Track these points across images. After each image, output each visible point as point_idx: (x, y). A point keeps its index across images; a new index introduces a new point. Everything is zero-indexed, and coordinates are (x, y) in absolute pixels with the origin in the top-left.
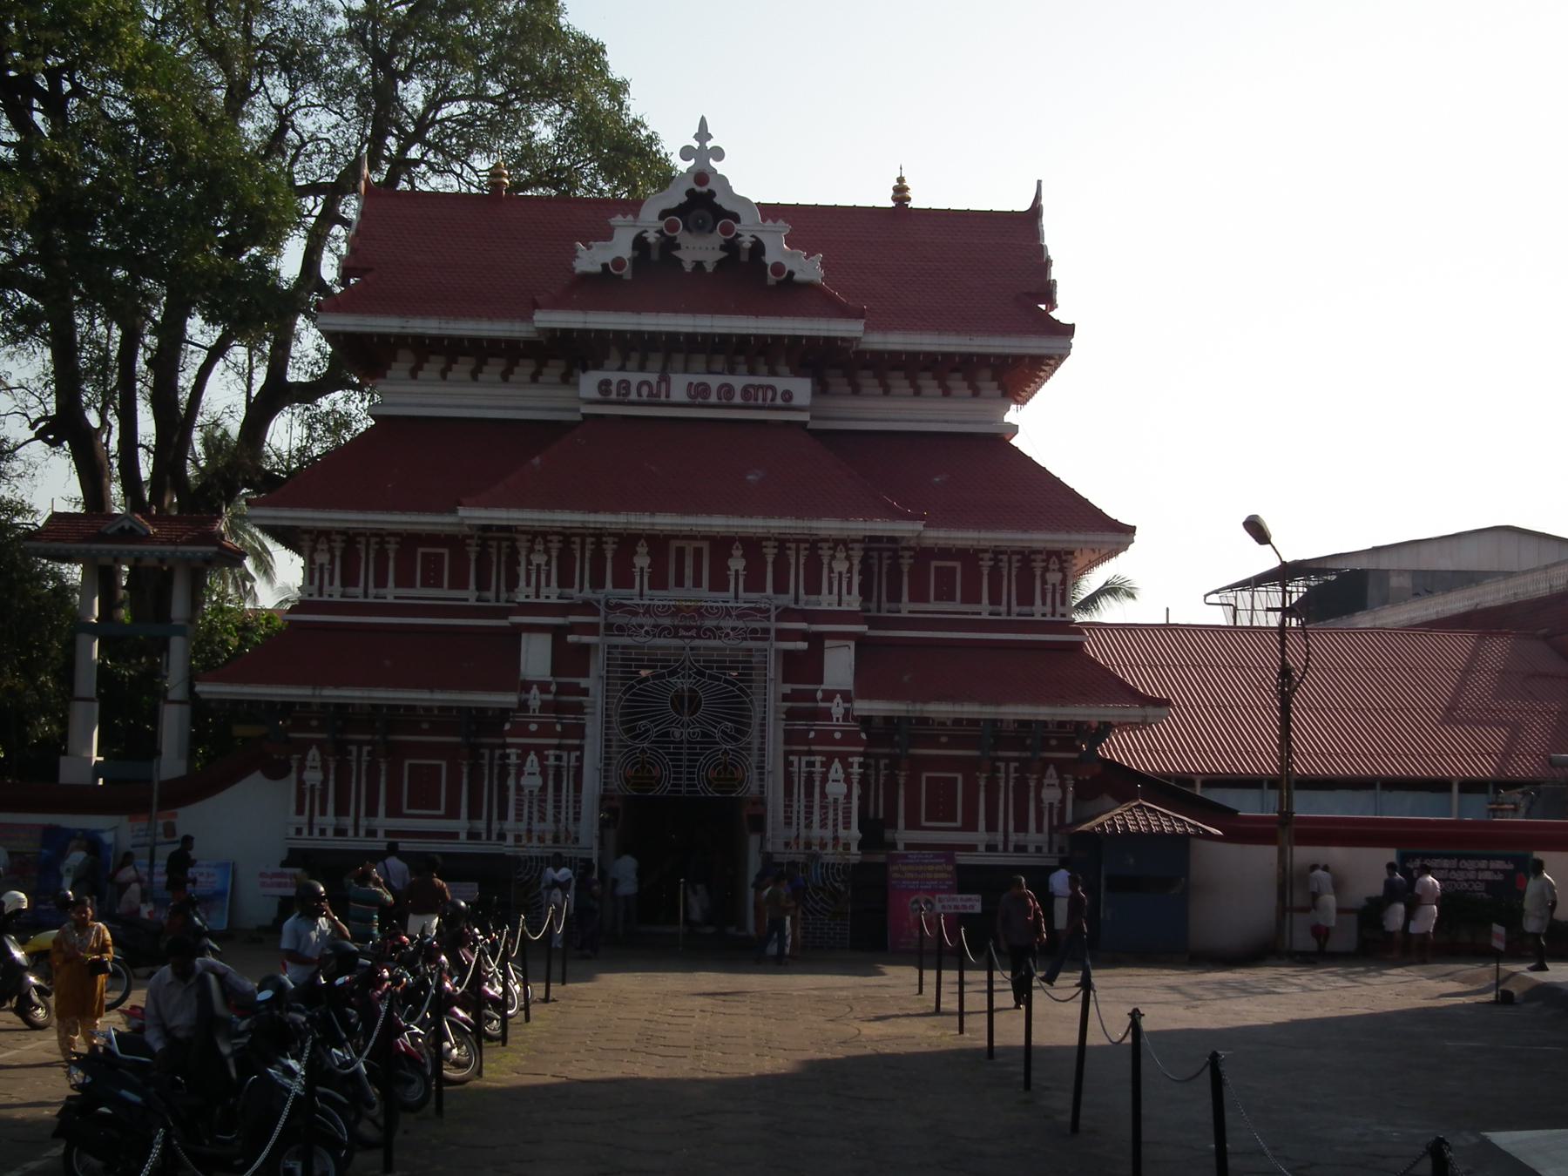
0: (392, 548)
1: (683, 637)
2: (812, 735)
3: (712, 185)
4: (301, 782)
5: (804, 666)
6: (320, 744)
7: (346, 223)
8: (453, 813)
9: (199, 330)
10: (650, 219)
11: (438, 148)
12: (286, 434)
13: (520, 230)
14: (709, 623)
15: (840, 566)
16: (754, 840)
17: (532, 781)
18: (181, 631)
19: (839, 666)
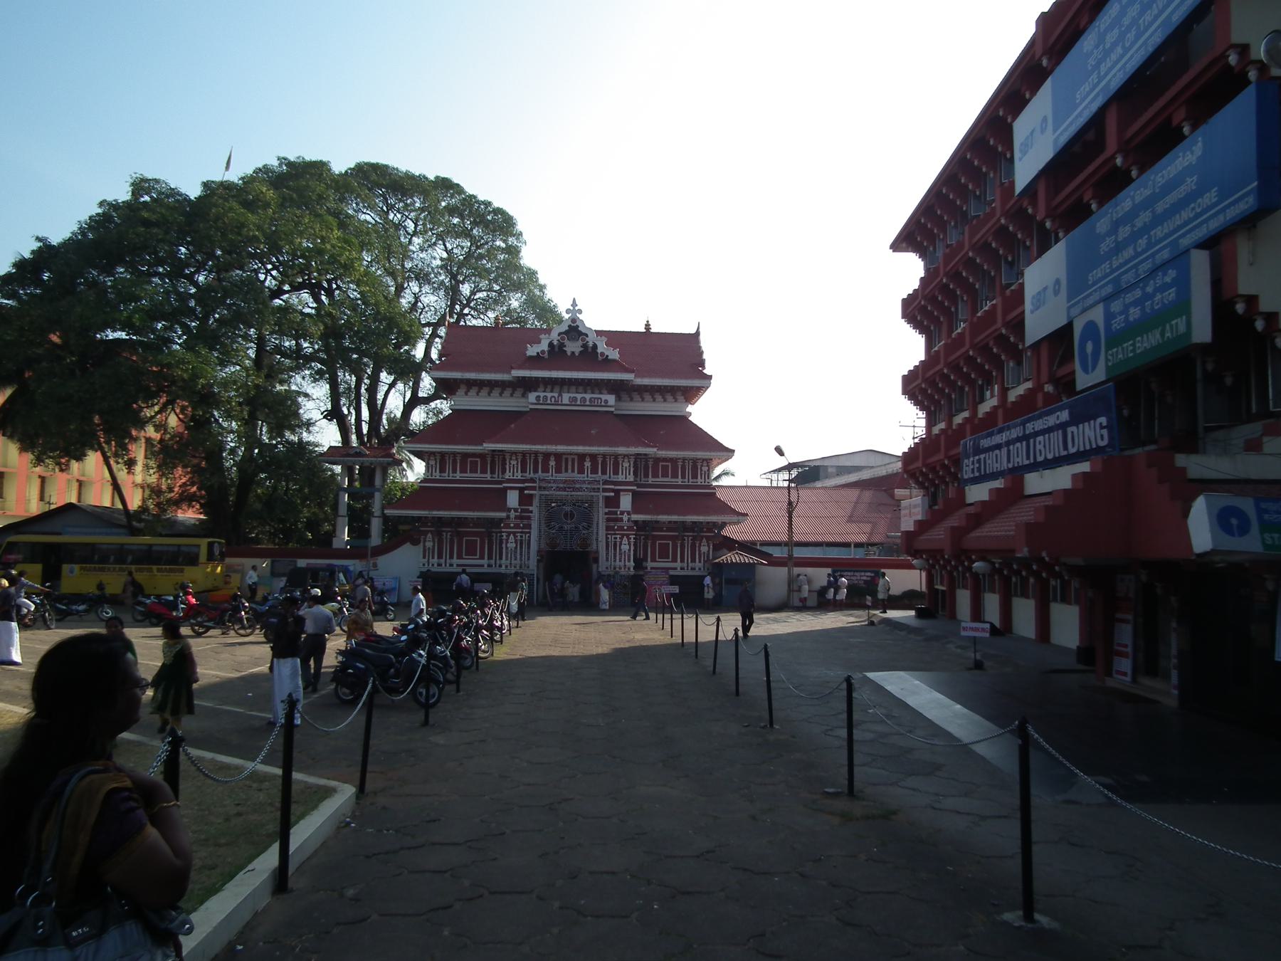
5: (613, 502)
7: (441, 337)
8: (482, 558)
9: (385, 377)
10: (554, 336)
11: (475, 309)
12: (418, 417)
13: (506, 339)
15: (626, 465)
16: (595, 566)
17: (512, 545)
18: (378, 490)
19: (626, 502)
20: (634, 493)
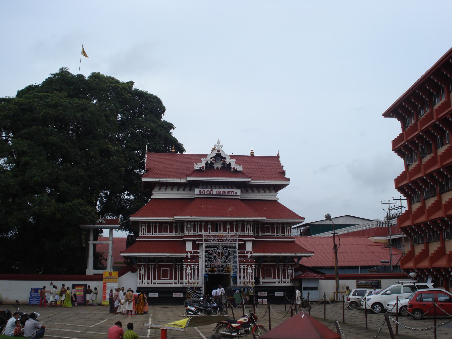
4: (140, 273)
5: (242, 247)
6: (144, 266)
8: (171, 279)
14: (225, 238)
17: (189, 272)
19: (249, 247)
20: (254, 243)
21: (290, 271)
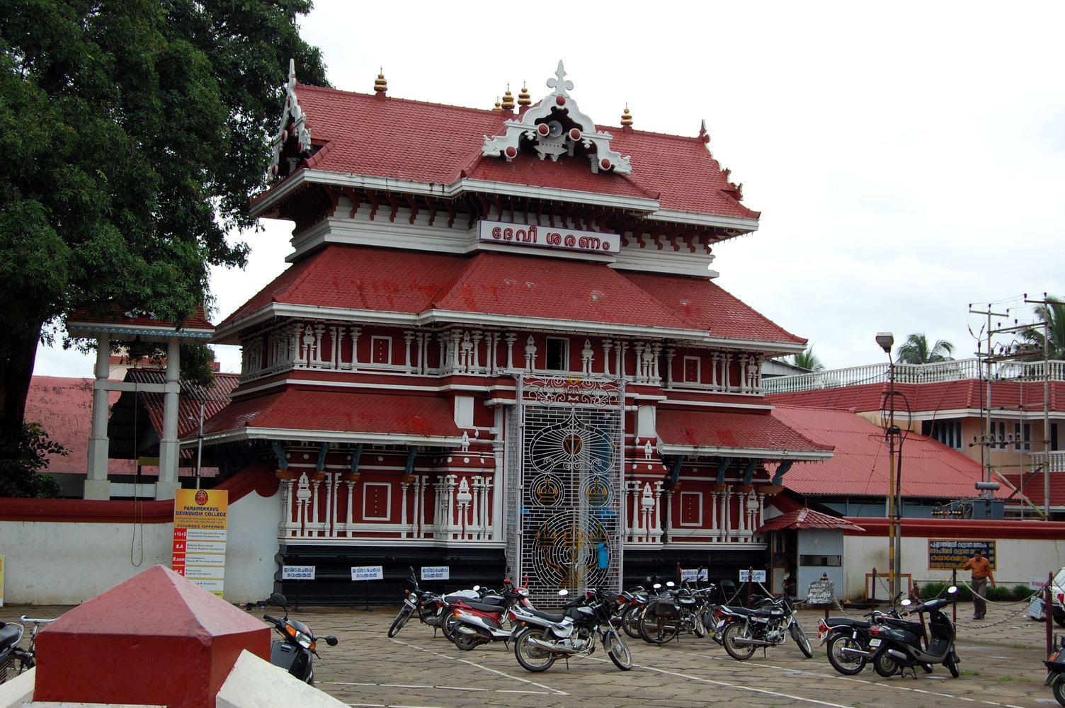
0: (355, 336)
1: (571, 402)
2: (635, 467)
3: (566, 106)
4: (295, 498)
6: (311, 474)
8: (396, 519)
14: (586, 392)
15: (648, 357)
17: (464, 497)
19: (647, 423)
21: (753, 505)
